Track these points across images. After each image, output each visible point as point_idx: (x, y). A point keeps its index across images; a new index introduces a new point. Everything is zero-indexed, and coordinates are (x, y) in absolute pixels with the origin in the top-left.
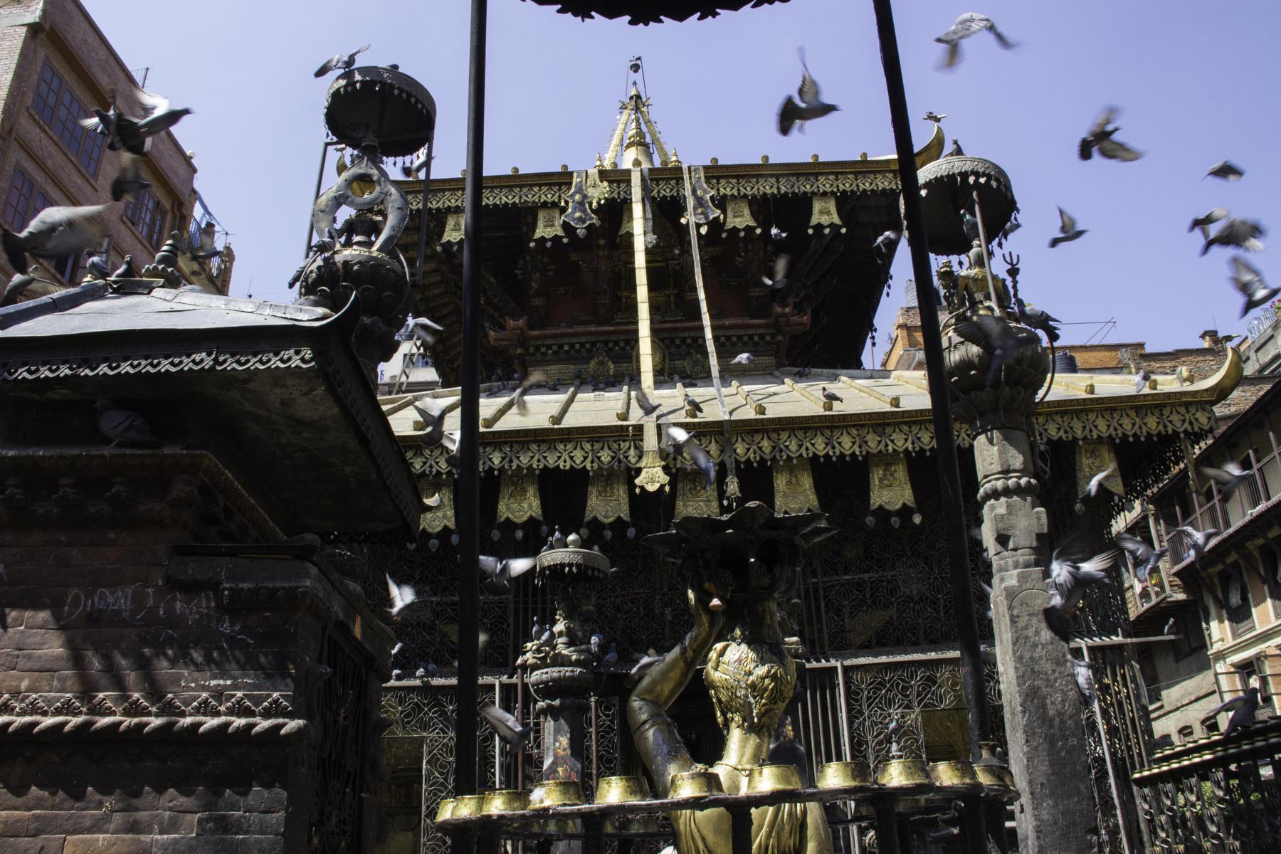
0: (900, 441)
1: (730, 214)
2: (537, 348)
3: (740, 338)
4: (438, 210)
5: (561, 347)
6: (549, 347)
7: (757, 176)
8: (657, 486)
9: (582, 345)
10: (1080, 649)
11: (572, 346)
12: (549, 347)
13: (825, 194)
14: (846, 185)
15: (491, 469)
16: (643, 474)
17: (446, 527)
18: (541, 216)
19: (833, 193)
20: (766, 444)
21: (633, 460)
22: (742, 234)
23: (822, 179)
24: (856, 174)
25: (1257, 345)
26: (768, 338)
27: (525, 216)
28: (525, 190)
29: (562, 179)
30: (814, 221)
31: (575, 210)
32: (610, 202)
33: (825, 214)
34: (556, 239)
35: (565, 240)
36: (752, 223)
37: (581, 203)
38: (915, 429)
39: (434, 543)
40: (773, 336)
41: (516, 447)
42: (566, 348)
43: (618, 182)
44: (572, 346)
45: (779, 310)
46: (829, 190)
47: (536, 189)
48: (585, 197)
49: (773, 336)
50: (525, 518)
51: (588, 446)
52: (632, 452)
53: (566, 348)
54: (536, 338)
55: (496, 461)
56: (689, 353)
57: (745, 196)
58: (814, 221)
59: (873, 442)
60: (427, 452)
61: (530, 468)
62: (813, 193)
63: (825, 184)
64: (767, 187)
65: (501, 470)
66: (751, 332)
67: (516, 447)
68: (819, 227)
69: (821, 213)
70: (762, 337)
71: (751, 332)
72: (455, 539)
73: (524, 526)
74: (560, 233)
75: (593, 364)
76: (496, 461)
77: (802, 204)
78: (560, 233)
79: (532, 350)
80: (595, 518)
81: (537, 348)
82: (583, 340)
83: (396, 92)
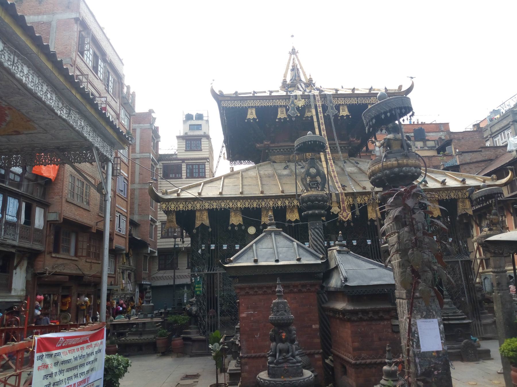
1: (341, 110)
2: (273, 150)
4: (246, 107)
6: (276, 150)
7: (350, 97)
9: (287, 149)
10: (458, 261)
11: (283, 149)
12: (276, 150)
15: (286, 206)
18: (279, 110)
20: (366, 198)
22: (345, 118)
23: (372, 98)
25: (491, 125)
26: (346, 148)
27: (275, 109)
28: (274, 101)
31: (292, 110)
34: (285, 118)
35: (288, 119)
37: (294, 107)
40: (348, 147)
41: (292, 199)
44: (283, 149)
45: (352, 139)
48: (295, 105)
50: (294, 220)
60: (265, 200)
64: (354, 101)
67: (292, 199)
70: (344, 147)
74: (286, 116)
75: (291, 156)
78: (286, 116)
81: (273, 150)
82: (287, 148)
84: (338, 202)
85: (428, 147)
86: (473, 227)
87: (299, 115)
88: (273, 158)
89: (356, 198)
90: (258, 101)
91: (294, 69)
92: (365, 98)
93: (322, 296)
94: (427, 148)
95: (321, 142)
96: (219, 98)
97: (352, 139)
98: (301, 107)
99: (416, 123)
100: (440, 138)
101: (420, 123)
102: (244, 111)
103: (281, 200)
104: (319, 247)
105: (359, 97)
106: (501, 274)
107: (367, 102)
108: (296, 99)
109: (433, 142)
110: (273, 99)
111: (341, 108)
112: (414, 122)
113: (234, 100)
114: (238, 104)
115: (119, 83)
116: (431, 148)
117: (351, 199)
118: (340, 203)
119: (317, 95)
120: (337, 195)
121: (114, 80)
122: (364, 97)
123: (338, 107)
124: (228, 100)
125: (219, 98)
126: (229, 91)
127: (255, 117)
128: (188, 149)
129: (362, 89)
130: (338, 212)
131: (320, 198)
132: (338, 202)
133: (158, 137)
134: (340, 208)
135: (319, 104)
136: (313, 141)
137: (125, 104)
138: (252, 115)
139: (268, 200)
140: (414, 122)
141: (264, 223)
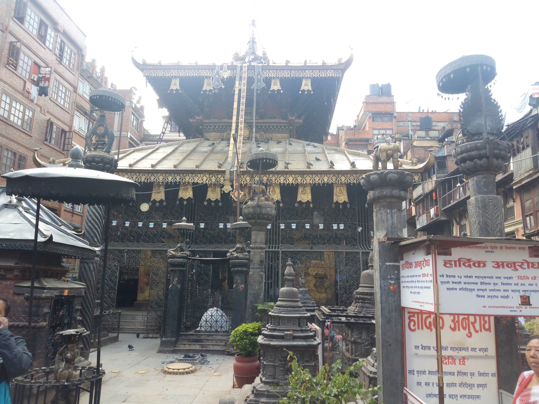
0: (308, 180)
1: (272, 84)
2: (207, 126)
3: (277, 127)
4: (168, 77)
5: (215, 126)
6: (211, 126)
7: (283, 70)
8: (228, 191)
9: (222, 126)
11: (219, 126)
12: (211, 126)
13: (307, 78)
14: (316, 74)
15: (176, 182)
16: (225, 187)
17: (162, 199)
18: (206, 81)
19: (310, 77)
21: (222, 181)
23: (307, 71)
24: (319, 70)
26: (287, 127)
27: (200, 81)
29: (212, 68)
30: (302, 89)
32: (230, 77)
33: (306, 86)
34: (210, 91)
36: (280, 88)
38: (314, 176)
39: (158, 204)
40: (289, 127)
41: (185, 175)
42: (217, 127)
43: (233, 70)
44: (219, 126)
46: (309, 76)
47: (204, 71)
48: (219, 76)
49: (289, 127)
50: (187, 198)
51: (208, 176)
52: (222, 179)
53: (217, 127)
54: (207, 123)
55: (178, 179)
56: (259, 131)
57: (278, 77)
58: (302, 89)
59: (299, 179)
60: (155, 175)
61: (189, 182)
62: (303, 77)
63: (308, 73)
64: (286, 74)
65: (179, 182)
66: (282, 125)
68: (304, 91)
69: (305, 85)
70: (285, 127)
71: (282, 125)
72: (165, 204)
73: (187, 200)
75: (225, 134)
76: (178, 179)
77: (299, 81)
79: (205, 127)
80: (209, 199)
81: (207, 126)
83: (110, 99)
84: (231, 181)
85: (431, 138)
86: (453, 226)
87: (223, 87)
88: (207, 135)
89: (252, 177)
90: (183, 71)
91: (253, 42)
92: (300, 71)
93: (87, 267)
94: (429, 138)
95: (109, 97)
96: (143, 67)
97: (290, 118)
98: (227, 78)
99: (426, 111)
100: (444, 128)
101: (430, 111)
102: (168, 81)
103: (173, 175)
104: (91, 213)
105: (293, 70)
106: (255, 250)
107: (301, 76)
108: (222, 69)
109: (437, 132)
110: (198, 70)
111: (273, 81)
112: (423, 110)
113: (157, 70)
114: (160, 74)
115: (79, 55)
116: (433, 139)
117: (248, 178)
118: (233, 181)
119: (245, 66)
120: (231, 173)
121: (71, 51)
122: (298, 70)
123: (268, 81)
124: (150, 69)
125: (143, 67)
126: (152, 60)
127: (179, 88)
128: (173, 130)
129: (297, 61)
130: (230, 192)
131: (97, 159)
132: (231, 181)
133: (142, 116)
134: (232, 186)
135: (245, 75)
136: (99, 95)
137: (89, 77)
138: (175, 86)
139: (159, 175)
140: (423, 110)
141: (154, 200)
